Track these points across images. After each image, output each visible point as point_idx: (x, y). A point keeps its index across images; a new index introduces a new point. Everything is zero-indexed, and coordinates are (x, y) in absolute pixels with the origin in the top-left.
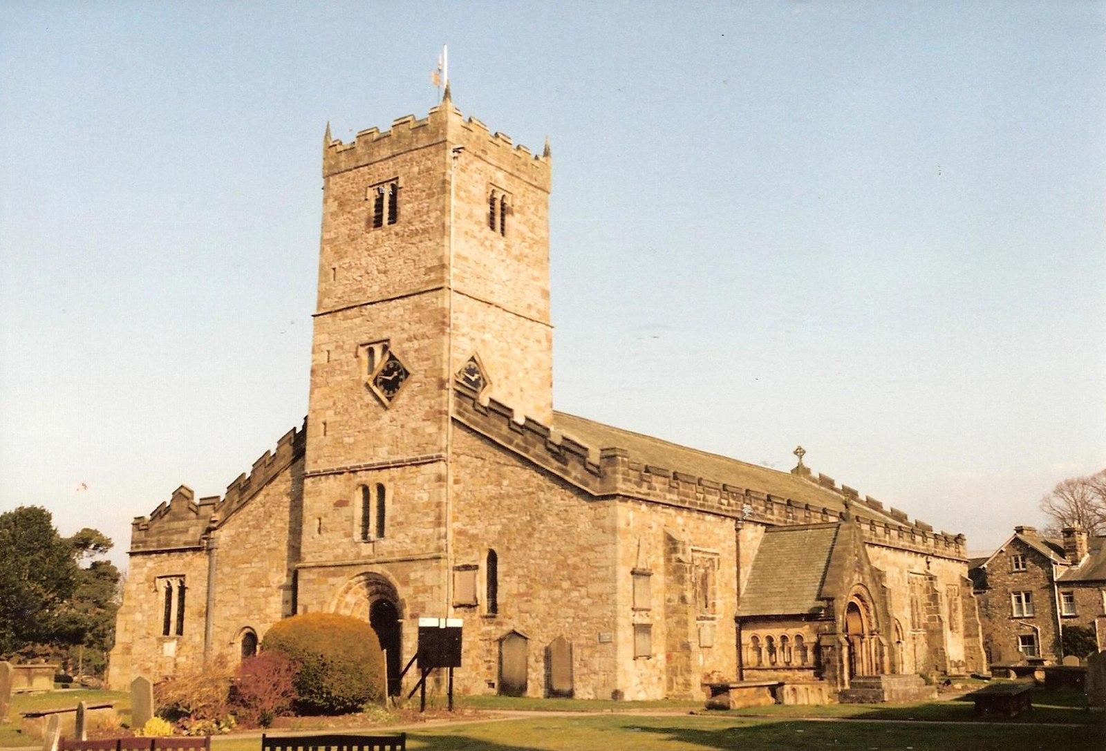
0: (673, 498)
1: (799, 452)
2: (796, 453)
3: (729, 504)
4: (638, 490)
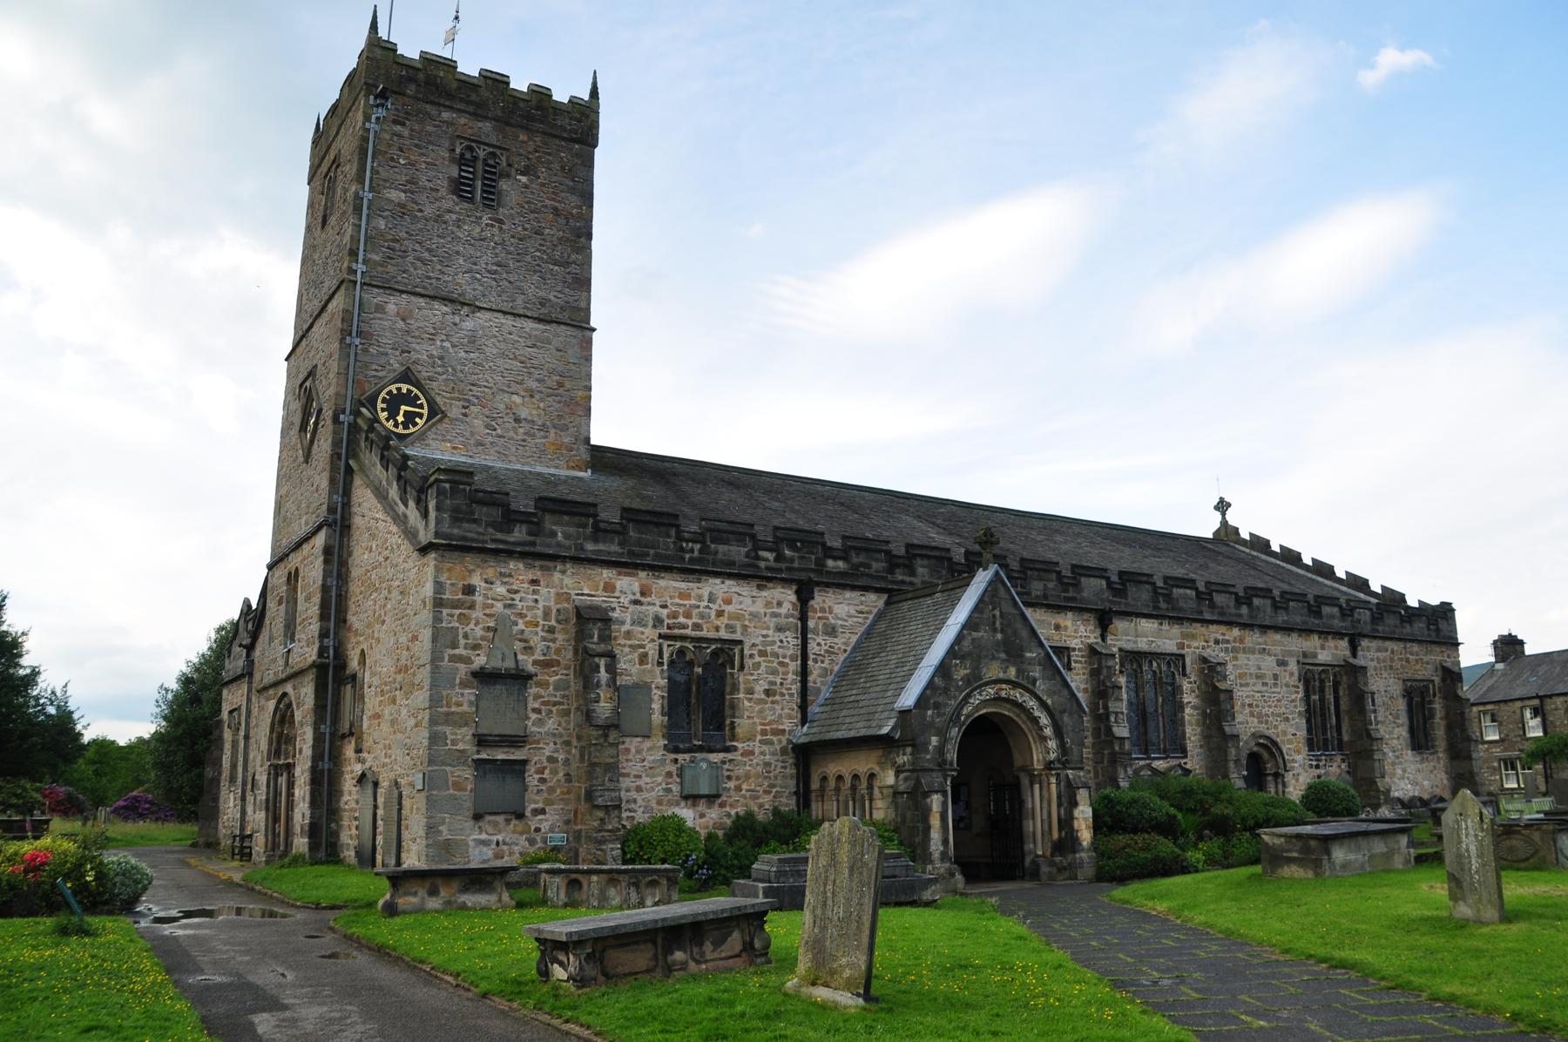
1: (1223, 506)
2: (1216, 508)
3: (779, 558)
4: (499, 536)
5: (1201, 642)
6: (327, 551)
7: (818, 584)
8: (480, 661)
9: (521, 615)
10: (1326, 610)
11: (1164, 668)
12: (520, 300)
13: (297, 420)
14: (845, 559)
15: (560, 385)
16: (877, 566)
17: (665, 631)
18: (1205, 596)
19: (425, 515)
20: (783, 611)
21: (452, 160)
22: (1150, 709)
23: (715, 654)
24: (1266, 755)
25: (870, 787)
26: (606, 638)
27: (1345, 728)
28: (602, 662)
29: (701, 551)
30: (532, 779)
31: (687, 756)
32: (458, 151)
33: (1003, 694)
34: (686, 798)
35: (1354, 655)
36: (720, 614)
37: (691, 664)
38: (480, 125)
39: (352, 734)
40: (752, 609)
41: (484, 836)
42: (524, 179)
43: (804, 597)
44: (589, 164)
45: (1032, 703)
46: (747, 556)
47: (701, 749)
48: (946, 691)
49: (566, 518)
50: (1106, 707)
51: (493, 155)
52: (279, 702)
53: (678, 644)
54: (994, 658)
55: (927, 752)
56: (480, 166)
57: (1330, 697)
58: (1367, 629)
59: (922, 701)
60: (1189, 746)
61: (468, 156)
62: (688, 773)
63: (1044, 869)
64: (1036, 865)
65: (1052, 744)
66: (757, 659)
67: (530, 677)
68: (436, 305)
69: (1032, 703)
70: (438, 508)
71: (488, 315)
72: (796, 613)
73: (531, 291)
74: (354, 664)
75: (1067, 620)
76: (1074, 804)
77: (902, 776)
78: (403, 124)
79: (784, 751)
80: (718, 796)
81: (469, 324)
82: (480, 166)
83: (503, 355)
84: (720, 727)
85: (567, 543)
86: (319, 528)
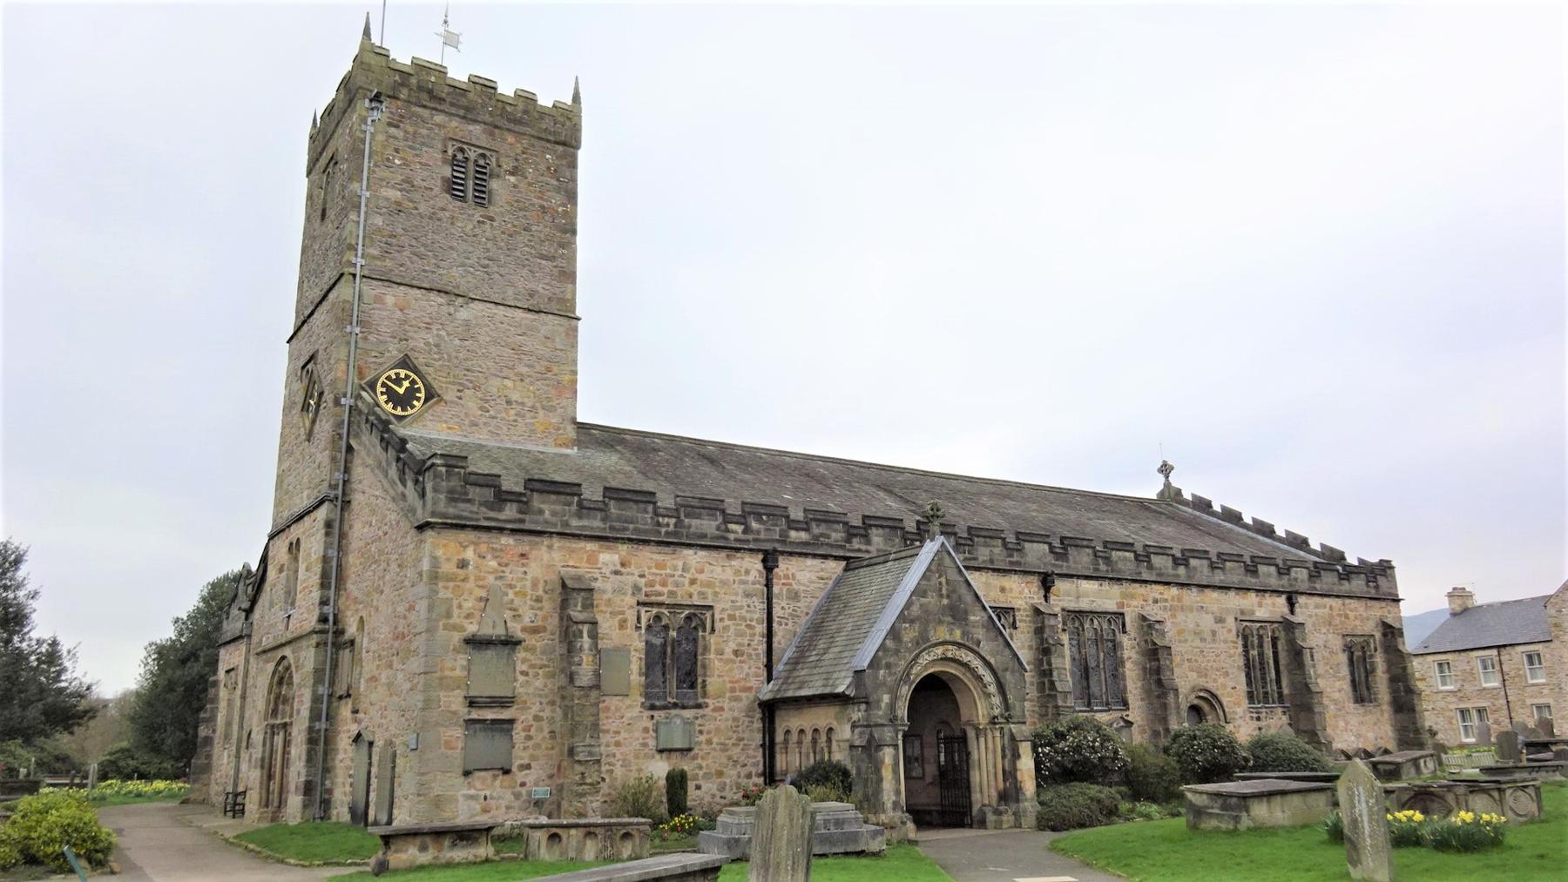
0: (595, 524)
1: (1166, 469)
3: (747, 530)
4: (492, 514)
5: (1137, 601)
6: (328, 525)
7: (782, 553)
8: (472, 629)
9: (511, 586)
10: (1262, 569)
11: (1105, 626)
12: (510, 292)
13: (300, 399)
14: (807, 530)
15: (549, 370)
16: (837, 535)
17: (643, 598)
18: (1143, 557)
19: (423, 495)
20: (751, 578)
21: (445, 161)
22: (1092, 664)
23: (688, 618)
24: (1206, 708)
25: (829, 740)
26: (589, 606)
27: (1284, 683)
28: (585, 629)
29: (676, 525)
30: (518, 733)
31: (662, 713)
32: (450, 152)
33: (949, 655)
34: (661, 751)
35: (1292, 612)
36: (693, 582)
37: (666, 628)
38: (471, 127)
39: (349, 696)
40: (723, 577)
41: (472, 792)
42: (512, 179)
43: (769, 562)
44: (573, 165)
45: (976, 663)
46: (718, 528)
47: (675, 706)
48: (897, 652)
49: (553, 497)
50: (1050, 664)
51: (483, 156)
52: (278, 664)
53: (655, 610)
54: (940, 622)
55: (879, 708)
56: (471, 166)
57: (1269, 652)
58: (1304, 587)
59: (874, 663)
60: (1131, 699)
61: (460, 156)
62: (662, 728)
63: (991, 817)
64: (982, 813)
65: (997, 700)
66: (727, 622)
67: (518, 643)
68: (433, 295)
69: (976, 663)
70: (435, 490)
71: (481, 306)
72: (763, 581)
73: (520, 285)
74: (352, 631)
75: (1013, 583)
76: (1016, 756)
77: (857, 731)
78: (397, 127)
79: (750, 709)
80: (690, 750)
81: (463, 314)
82: (471, 166)
83: (495, 342)
84: (693, 686)
85: (554, 520)
86: (321, 503)
